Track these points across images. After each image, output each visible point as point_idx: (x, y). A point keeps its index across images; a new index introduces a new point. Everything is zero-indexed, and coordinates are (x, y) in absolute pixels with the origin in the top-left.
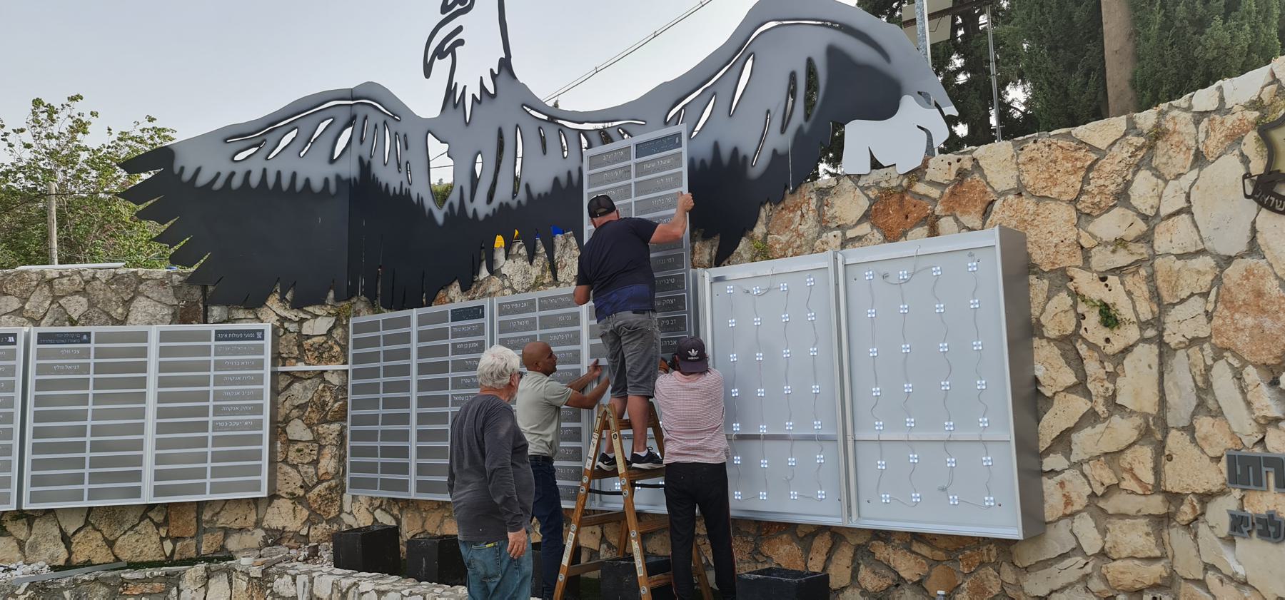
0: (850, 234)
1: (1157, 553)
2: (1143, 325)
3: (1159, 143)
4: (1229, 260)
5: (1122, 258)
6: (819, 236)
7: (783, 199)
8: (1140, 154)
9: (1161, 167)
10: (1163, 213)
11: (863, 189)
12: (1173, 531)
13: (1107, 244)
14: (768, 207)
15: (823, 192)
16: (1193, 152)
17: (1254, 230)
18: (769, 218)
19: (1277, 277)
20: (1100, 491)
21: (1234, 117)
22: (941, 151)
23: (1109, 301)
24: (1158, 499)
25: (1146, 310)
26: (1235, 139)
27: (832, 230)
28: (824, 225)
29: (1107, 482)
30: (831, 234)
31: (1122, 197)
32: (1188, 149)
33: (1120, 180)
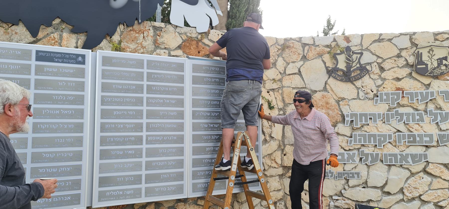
0: (173, 53)
1: (281, 188)
2: (280, 110)
3: (287, 50)
4: (316, 91)
5: (275, 86)
6: (155, 50)
7: (132, 26)
8: (280, 51)
9: (286, 59)
10: (287, 72)
11: (180, 34)
12: (284, 180)
13: (270, 80)
14: (122, 27)
15: (155, 28)
16: (301, 56)
17: (326, 83)
18: (122, 32)
19: (334, 99)
20: (267, 168)
21: (320, 48)
22: (216, 28)
23: (270, 100)
24: (281, 169)
25: (281, 105)
26: (320, 55)
27: (163, 49)
28: (157, 45)
29: (269, 165)
30: (162, 51)
31: (275, 64)
32: (299, 54)
33: (274, 59)
